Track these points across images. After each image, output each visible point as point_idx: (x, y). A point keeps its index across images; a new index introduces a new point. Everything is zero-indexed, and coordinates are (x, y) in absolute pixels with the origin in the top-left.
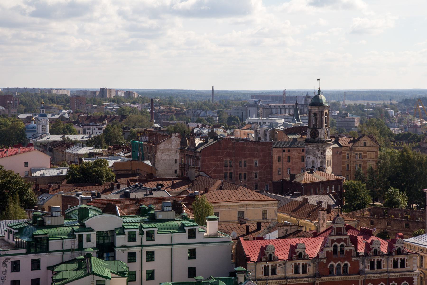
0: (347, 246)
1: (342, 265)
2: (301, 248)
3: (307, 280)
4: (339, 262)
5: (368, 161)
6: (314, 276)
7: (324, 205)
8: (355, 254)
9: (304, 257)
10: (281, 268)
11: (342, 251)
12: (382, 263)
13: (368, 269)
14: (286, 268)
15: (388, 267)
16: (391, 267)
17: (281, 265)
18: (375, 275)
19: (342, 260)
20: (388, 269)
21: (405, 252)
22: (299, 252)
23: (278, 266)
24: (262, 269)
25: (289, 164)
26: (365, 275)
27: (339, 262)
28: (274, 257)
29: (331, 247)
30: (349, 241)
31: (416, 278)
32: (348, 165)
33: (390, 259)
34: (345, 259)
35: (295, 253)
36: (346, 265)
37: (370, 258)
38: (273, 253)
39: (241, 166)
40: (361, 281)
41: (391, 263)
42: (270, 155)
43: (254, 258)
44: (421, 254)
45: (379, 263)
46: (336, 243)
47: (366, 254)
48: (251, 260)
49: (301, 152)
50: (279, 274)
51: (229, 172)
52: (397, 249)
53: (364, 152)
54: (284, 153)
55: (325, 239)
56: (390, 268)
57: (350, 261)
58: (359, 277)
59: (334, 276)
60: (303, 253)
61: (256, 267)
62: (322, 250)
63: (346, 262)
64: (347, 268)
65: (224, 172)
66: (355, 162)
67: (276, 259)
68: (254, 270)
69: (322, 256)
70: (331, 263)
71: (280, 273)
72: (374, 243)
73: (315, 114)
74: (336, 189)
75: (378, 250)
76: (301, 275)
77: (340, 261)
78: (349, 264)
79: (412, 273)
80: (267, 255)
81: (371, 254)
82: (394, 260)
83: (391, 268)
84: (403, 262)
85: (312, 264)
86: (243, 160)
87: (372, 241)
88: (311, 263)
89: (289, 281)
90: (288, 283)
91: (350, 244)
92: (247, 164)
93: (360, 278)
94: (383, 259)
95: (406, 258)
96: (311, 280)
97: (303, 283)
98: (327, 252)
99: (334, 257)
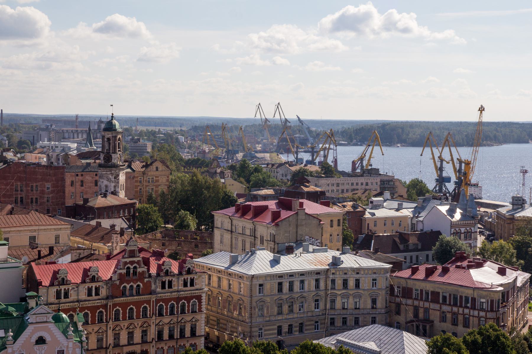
1: (135, 286)
4: (132, 284)
5: (160, 185)
6: (107, 298)
7: (117, 228)
8: (147, 275)
9: (97, 280)
11: (135, 273)
12: (173, 283)
14: (79, 291)
17: (74, 288)
18: (166, 294)
19: (135, 281)
20: (178, 289)
21: (194, 272)
25: (83, 188)
26: (156, 294)
27: (132, 284)
28: (67, 281)
30: (142, 263)
31: (204, 295)
32: (140, 189)
33: (181, 279)
35: (88, 276)
36: (138, 286)
37: (161, 278)
38: (66, 276)
39: (32, 191)
40: (153, 301)
41: (181, 283)
42: (63, 180)
43: (46, 282)
44: (209, 273)
45: (170, 282)
46: (129, 265)
47: (158, 275)
48: (43, 284)
49: (94, 176)
51: (19, 196)
52: (187, 269)
53: (156, 177)
54: (77, 177)
55: (119, 261)
56: (180, 288)
57: (142, 282)
58: (151, 297)
59: (127, 297)
60: (96, 276)
61: (48, 291)
62: (115, 272)
63: (139, 283)
64: (139, 289)
65: (14, 196)
66: (147, 186)
67: (68, 282)
68: (46, 295)
69: (115, 278)
70: (123, 285)
71: (73, 296)
72: (165, 264)
73: (109, 139)
74: (129, 212)
75: (170, 271)
76: (94, 297)
77: (133, 282)
79: (201, 291)
80: (60, 279)
81: (162, 274)
82: (184, 279)
83: (181, 287)
84: (192, 280)
85: (105, 286)
86: (35, 184)
87: (164, 262)
88: (104, 285)
90: (81, 306)
91: (142, 265)
92: (39, 189)
94: (174, 279)
95: (195, 277)
98: (121, 274)
99: (127, 278)
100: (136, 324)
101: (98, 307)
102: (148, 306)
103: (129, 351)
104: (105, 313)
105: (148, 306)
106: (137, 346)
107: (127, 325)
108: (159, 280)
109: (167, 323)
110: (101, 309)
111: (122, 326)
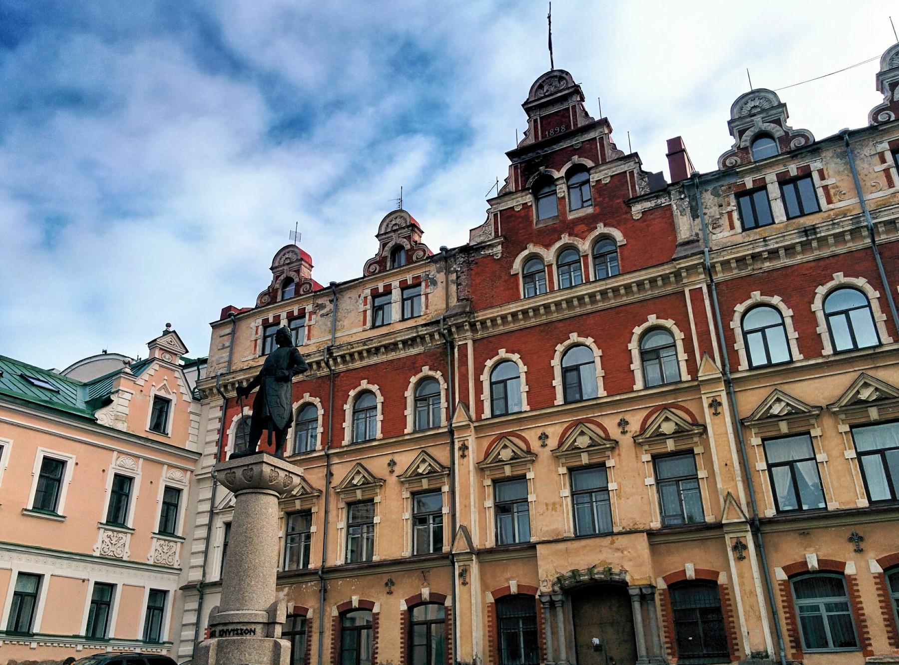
0: (597, 165)
1: (585, 246)
2: (395, 228)
3: (413, 340)
4: (565, 239)
10: (322, 316)
13: (732, 227)
14: (340, 315)
15: (858, 190)
16: (883, 182)
20: (862, 202)
22: (390, 245)
23: (311, 313)
24: (257, 333)
27: (565, 239)
29: (524, 190)
34: (589, 222)
40: (696, 294)
50: (312, 341)
63: (601, 229)
68: (227, 344)
78: (618, 235)
85: (441, 277)
88: (438, 272)
89: (343, 357)
90: (341, 367)
93: (684, 274)
96: (432, 335)
97: (402, 354)
100: (611, 425)
101: (413, 365)
102: (669, 323)
103: (575, 573)
104: (443, 386)
105: (669, 323)
106: (621, 541)
107: (560, 429)
108: (716, 194)
109: (823, 403)
110: (426, 371)
111: (532, 436)
